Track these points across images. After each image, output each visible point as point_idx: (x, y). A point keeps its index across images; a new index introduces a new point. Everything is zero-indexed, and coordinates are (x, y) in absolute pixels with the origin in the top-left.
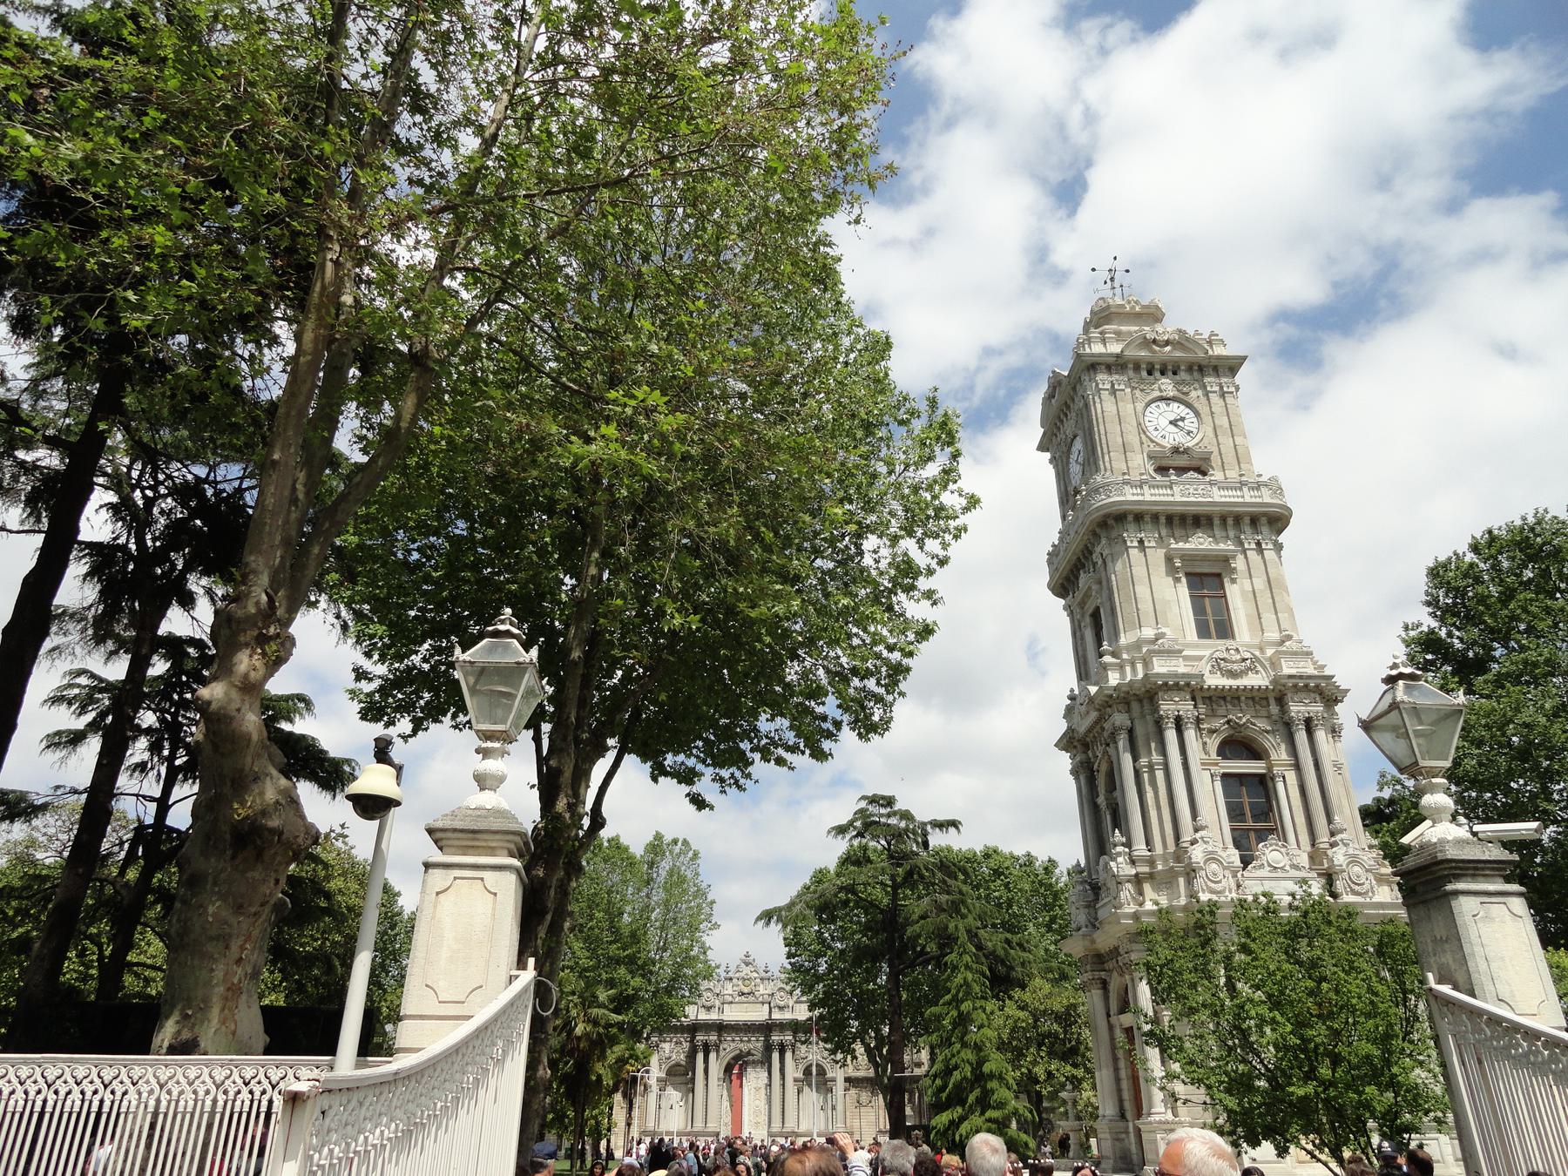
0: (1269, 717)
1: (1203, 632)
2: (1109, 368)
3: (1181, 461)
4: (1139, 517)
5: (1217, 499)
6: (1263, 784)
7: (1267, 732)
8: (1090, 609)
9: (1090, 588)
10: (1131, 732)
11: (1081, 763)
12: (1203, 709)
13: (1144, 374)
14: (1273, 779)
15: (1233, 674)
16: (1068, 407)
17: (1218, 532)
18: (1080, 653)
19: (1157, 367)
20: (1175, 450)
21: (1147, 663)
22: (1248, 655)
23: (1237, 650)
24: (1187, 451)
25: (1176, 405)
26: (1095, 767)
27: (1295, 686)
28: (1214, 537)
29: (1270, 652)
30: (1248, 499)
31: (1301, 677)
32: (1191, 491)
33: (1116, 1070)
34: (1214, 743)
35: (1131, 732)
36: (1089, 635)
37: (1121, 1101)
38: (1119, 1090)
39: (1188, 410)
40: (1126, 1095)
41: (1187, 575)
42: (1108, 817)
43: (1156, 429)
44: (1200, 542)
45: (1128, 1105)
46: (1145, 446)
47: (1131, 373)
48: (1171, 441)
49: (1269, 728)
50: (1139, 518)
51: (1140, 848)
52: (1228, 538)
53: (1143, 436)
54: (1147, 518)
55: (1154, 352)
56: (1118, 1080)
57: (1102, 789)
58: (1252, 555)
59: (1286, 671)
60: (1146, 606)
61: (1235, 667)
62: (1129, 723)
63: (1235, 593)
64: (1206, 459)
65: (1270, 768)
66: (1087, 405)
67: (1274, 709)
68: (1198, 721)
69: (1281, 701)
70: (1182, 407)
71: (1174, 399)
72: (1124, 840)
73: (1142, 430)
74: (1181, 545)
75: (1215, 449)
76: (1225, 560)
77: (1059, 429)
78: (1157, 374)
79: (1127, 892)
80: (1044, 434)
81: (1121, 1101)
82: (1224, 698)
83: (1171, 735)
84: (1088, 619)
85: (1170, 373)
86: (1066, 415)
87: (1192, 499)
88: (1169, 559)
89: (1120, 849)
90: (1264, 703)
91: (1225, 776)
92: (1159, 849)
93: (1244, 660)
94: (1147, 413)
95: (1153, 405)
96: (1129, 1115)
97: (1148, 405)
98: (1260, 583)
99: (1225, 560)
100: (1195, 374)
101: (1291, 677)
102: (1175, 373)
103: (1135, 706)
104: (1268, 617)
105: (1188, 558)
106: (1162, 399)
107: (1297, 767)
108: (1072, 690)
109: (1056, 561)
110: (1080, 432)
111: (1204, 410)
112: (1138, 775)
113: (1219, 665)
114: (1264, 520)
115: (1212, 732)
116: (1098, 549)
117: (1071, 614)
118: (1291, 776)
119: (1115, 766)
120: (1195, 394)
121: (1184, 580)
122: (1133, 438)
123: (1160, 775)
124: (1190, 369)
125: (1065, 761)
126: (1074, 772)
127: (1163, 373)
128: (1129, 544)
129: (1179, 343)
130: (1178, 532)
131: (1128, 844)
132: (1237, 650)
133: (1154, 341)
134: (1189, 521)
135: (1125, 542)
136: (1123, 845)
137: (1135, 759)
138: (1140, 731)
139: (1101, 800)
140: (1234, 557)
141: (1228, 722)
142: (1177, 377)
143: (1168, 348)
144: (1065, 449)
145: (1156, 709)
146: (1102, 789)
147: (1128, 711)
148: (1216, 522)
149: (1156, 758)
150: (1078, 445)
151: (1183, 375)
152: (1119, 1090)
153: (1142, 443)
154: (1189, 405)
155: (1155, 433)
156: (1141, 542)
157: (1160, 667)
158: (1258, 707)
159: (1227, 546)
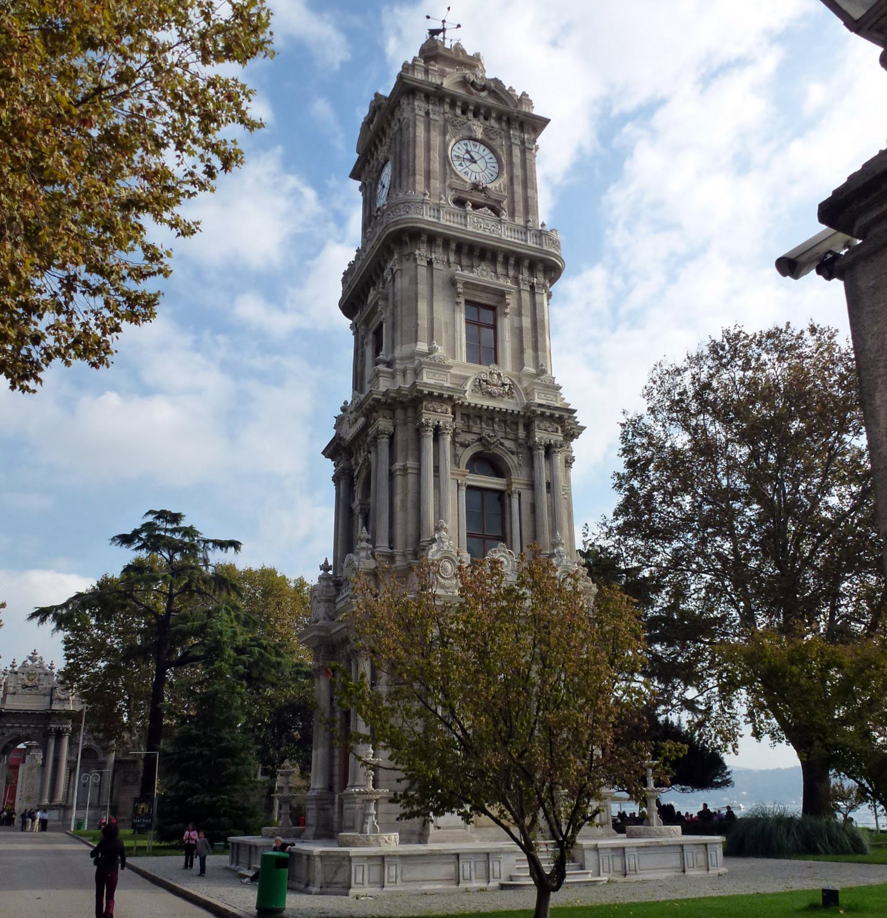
0: (516, 440)
2: (428, 97)
3: (479, 198)
4: (432, 238)
5: (504, 237)
6: (501, 496)
7: (513, 453)
8: (374, 326)
9: (376, 304)
10: (392, 437)
11: (343, 468)
12: (459, 423)
13: (459, 111)
14: (510, 496)
15: (491, 395)
16: (384, 132)
17: (500, 269)
18: (359, 370)
19: (471, 108)
20: (475, 187)
21: (417, 373)
22: (508, 381)
23: (499, 375)
24: (484, 190)
25: (482, 147)
26: (356, 473)
27: (543, 414)
28: (495, 272)
29: (525, 384)
30: (530, 243)
31: (549, 407)
33: (332, 748)
34: (466, 455)
35: (392, 437)
36: (369, 350)
37: (331, 775)
38: (331, 766)
39: (491, 155)
40: (336, 771)
41: (468, 302)
42: (360, 520)
44: (482, 275)
45: (336, 779)
47: (447, 108)
49: (515, 449)
51: (383, 545)
52: (507, 276)
54: (440, 242)
55: (472, 94)
56: (331, 757)
57: (358, 496)
58: (526, 296)
59: (538, 401)
60: (423, 323)
61: (495, 389)
62: (392, 429)
63: (506, 325)
65: (509, 485)
66: (400, 129)
67: (522, 433)
68: (455, 434)
69: (528, 427)
70: (487, 151)
71: (481, 142)
72: (369, 537)
73: (446, 161)
74: (466, 273)
76: (501, 294)
77: (372, 155)
78: (470, 115)
80: (359, 159)
81: (331, 775)
82: (480, 418)
83: (429, 443)
84: (371, 336)
85: (482, 118)
86: (381, 141)
88: (453, 283)
89: (364, 544)
90: (515, 427)
91: (470, 488)
92: (398, 550)
93: (504, 385)
95: (462, 142)
96: (336, 788)
98: (527, 322)
99: (501, 294)
100: (504, 124)
101: (540, 405)
102: (486, 119)
103: (399, 413)
104: (529, 353)
106: (470, 138)
107: (532, 486)
108: (346, 403)
109: (350, 279)
110: (391, 157)
112: (391, 475)
113: (480, 385)
114: (540, 266)
115: (465, 446)
116: (390, 265)
117: (356, 333)
118: (526, 496)
119: (373, 467)
120: (499, 142)
121: (463, 305)
122: (436, 166)
123: (411, 479)
124: (499, 119)
125: (329, 467)
126: (336, 479)
127: (475, 115)
128: (419, 262)
129: (494, 91)
130: (465, 262)
131: (372, 541)
132: (499, 375)
133: (473, 84)
134: (477, 253)
135: (415, 260)
136: (368, 541)
139: (356, 504)
140: (510, 293)
141: (480, 440)
142: (487, 123)
143: (484, 94)
144: (375, 175)
145: (418, 416)
146: (358, 496)
147: (393, 418)
148: (500, 258)
149: (411, 463)
150: (388, 171)
151: (493, 123)
152: (331, 766)
154: (493, 151)
155: (460, 168)
157: (428, 379)
158: (508, 430)
159: (506, 283)
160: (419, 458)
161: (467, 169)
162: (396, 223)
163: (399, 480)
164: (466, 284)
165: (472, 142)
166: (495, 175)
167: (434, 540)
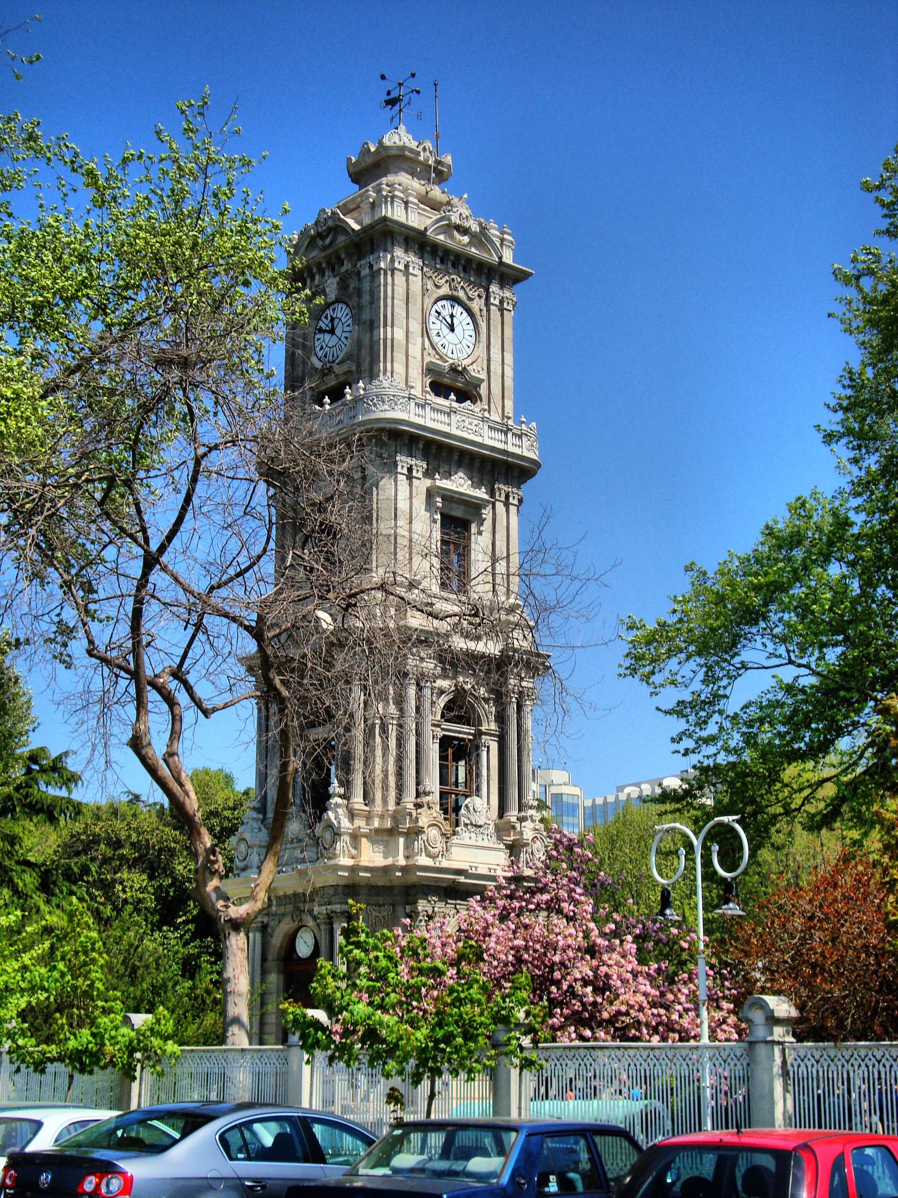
32: (466, 424)
39: (469, 320)
46: (426, 353)
53: (426, 340)
58: (500, 507)
64: (477, 384)
75: (483, 376)
79: (343, 844)
92: (378, 808)
100: (483, 277)
105: (450, 498)
111: (483, 326)
118: (494, 746)
128: (399, 470)
143: (466, 239)
153: (424, 349)
156: (410, 470)
159: (481, 493)
161: (443, 341)
166: (472, 347)
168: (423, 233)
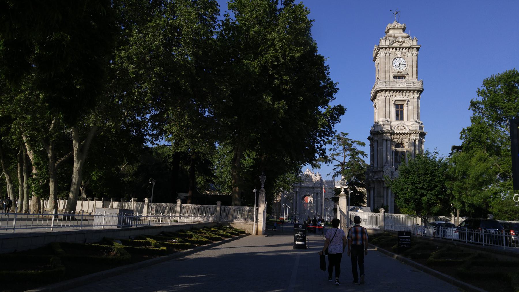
1: (397, 119)
3: (399, 75)
22: (404, 125)
35: (377, 141)
43: (395, 66)
44: (399, 97)
48: (399, 69)
50: (386, 91)
63: (405, 109)
70: (403, 59)
78: (398, 50)
83: (384, 143)
87: (400, 86)
94: (394, 61)
95: (396, 59)
97: (394, 59)
106: (398, 57)
112: (378, 150)
127: (399, 50)
137: (378, 147)
138: (379, 141)
155: (395, 67)
160: (383, 146)
162: (377, 88)
163: (379, 151)
164: (395, 101)
165: (399, 58)
167: (385, 166)
168: (388, 46)
